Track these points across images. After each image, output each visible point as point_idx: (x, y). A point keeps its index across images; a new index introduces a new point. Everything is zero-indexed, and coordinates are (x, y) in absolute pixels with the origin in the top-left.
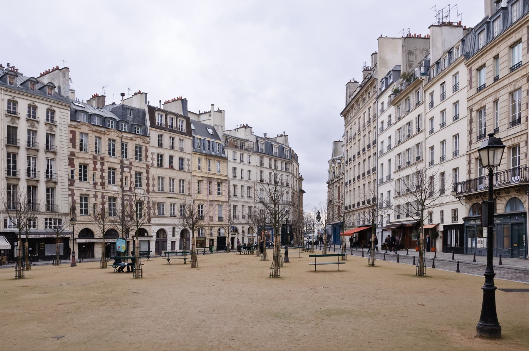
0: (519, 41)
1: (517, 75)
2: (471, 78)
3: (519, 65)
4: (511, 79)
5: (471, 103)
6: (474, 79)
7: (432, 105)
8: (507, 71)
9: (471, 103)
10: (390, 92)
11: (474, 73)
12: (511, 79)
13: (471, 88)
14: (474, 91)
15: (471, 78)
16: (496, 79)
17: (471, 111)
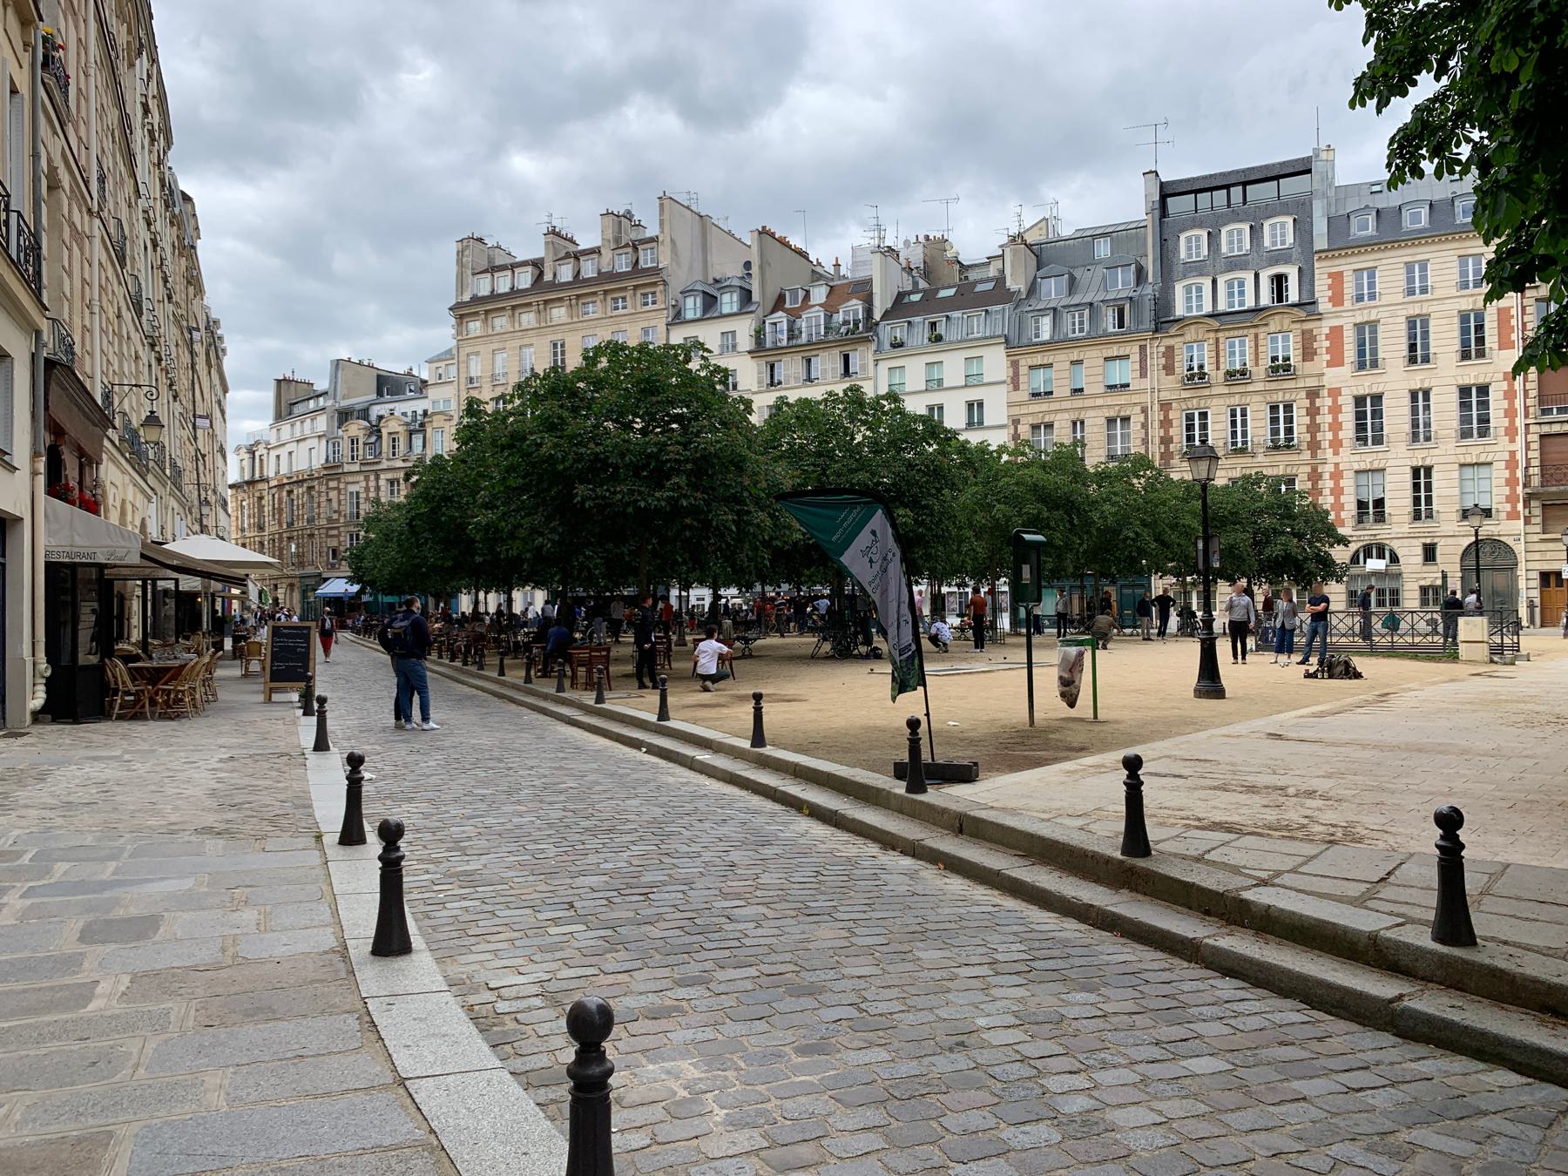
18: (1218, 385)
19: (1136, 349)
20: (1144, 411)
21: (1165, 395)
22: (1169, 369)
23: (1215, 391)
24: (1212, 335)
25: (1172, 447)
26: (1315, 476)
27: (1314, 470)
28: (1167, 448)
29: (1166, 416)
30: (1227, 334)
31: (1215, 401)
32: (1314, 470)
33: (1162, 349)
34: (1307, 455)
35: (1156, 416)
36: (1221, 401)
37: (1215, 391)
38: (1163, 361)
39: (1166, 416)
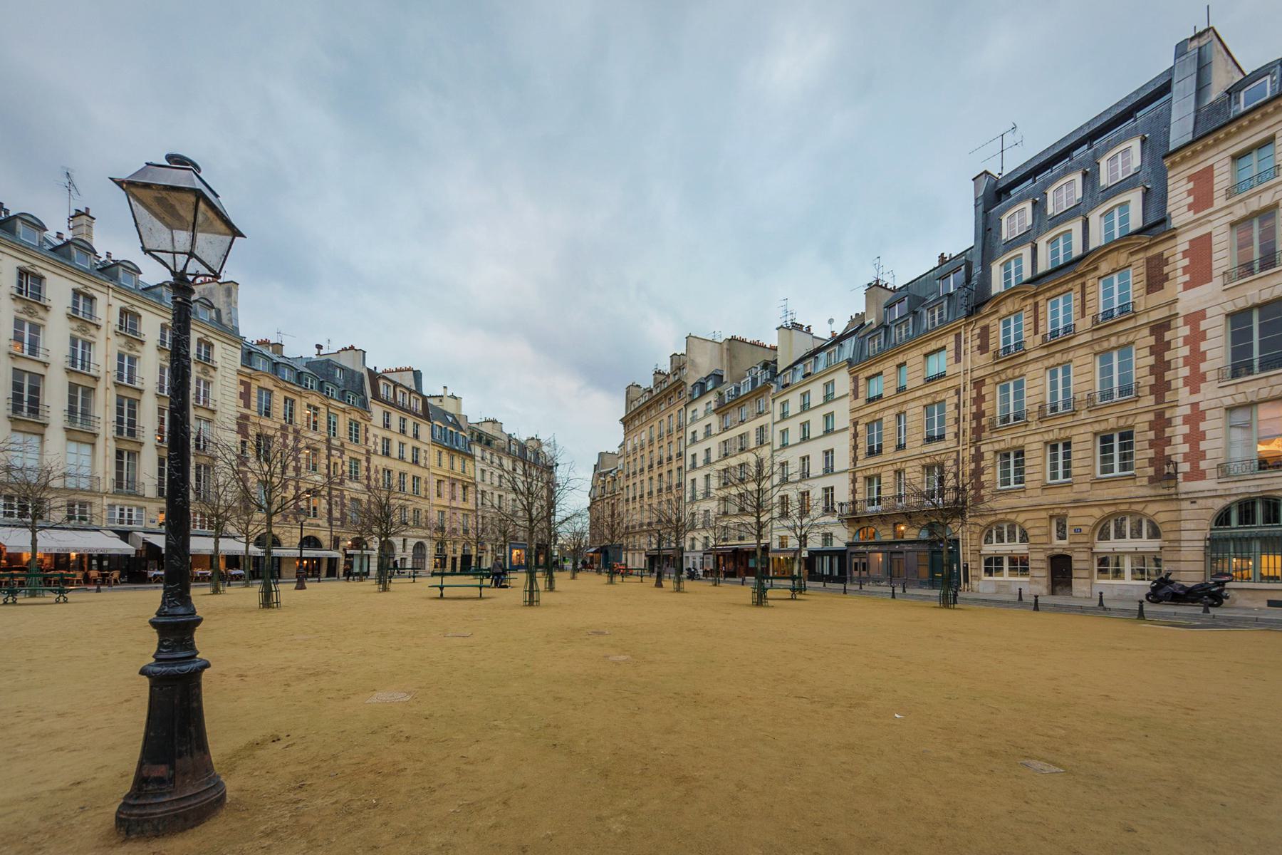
0: (943, 348)
1: (937, 387)
2: (856, 387)
3: (942, 376)
4: (927, 391)
5: (856, 415)
6: (861, 389)
7: (784, 416)
8: (920, 382)
9: (856, 415)
10: (712, 398)
11: (862, 382)
12: (927, 391)
13: (856, 397)
14: (861, 402)
15: (856, 387)
16: (901, 390)
17: (856, 424)
18: (1035, 349)
19: (952, 338)
20: (958, 393)
21: (976, 374)
22: (983, 348)
23: (1031, 356)
24: (1030, 301)
25: (984, 421)
26: (1161, 423)
27: (1160, 415)
28: (979, 422)
29: (979, 393)
30: (1048, 295)
31: (1031, 367)
32: (1160, 415)
33: (977, 331)
34: (1149, 401)
35: (969, 394)
36: (1039, 365)
37: (1031, 356)
38: (978, 342)
39: (979, 393)
